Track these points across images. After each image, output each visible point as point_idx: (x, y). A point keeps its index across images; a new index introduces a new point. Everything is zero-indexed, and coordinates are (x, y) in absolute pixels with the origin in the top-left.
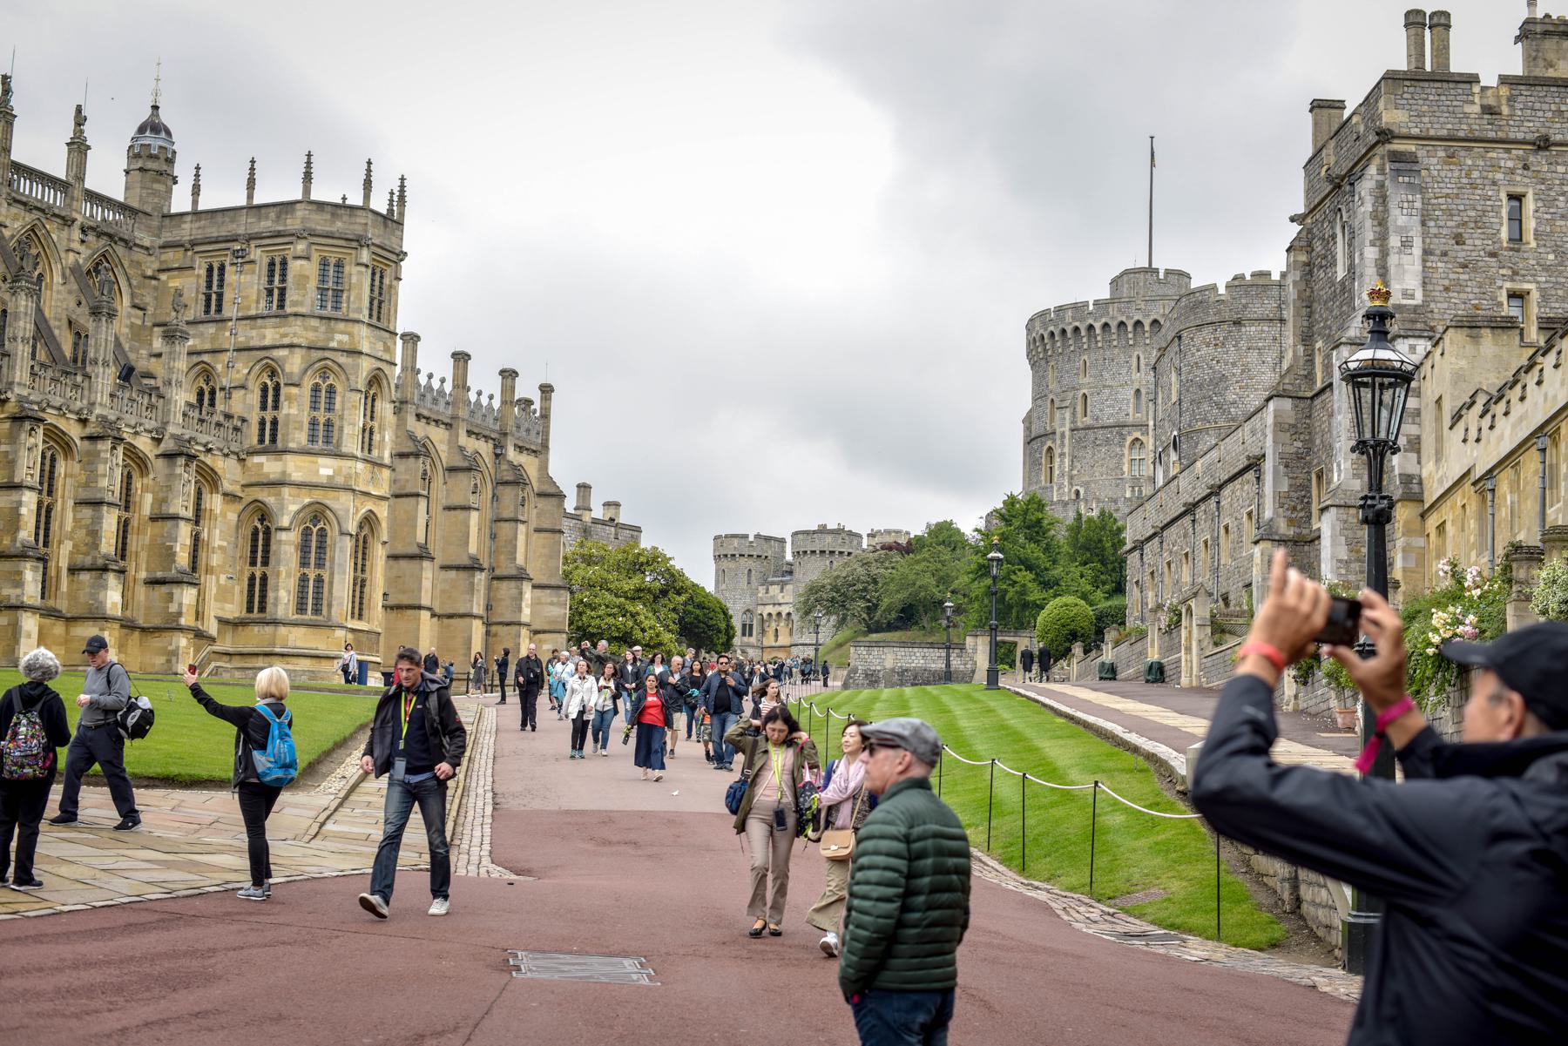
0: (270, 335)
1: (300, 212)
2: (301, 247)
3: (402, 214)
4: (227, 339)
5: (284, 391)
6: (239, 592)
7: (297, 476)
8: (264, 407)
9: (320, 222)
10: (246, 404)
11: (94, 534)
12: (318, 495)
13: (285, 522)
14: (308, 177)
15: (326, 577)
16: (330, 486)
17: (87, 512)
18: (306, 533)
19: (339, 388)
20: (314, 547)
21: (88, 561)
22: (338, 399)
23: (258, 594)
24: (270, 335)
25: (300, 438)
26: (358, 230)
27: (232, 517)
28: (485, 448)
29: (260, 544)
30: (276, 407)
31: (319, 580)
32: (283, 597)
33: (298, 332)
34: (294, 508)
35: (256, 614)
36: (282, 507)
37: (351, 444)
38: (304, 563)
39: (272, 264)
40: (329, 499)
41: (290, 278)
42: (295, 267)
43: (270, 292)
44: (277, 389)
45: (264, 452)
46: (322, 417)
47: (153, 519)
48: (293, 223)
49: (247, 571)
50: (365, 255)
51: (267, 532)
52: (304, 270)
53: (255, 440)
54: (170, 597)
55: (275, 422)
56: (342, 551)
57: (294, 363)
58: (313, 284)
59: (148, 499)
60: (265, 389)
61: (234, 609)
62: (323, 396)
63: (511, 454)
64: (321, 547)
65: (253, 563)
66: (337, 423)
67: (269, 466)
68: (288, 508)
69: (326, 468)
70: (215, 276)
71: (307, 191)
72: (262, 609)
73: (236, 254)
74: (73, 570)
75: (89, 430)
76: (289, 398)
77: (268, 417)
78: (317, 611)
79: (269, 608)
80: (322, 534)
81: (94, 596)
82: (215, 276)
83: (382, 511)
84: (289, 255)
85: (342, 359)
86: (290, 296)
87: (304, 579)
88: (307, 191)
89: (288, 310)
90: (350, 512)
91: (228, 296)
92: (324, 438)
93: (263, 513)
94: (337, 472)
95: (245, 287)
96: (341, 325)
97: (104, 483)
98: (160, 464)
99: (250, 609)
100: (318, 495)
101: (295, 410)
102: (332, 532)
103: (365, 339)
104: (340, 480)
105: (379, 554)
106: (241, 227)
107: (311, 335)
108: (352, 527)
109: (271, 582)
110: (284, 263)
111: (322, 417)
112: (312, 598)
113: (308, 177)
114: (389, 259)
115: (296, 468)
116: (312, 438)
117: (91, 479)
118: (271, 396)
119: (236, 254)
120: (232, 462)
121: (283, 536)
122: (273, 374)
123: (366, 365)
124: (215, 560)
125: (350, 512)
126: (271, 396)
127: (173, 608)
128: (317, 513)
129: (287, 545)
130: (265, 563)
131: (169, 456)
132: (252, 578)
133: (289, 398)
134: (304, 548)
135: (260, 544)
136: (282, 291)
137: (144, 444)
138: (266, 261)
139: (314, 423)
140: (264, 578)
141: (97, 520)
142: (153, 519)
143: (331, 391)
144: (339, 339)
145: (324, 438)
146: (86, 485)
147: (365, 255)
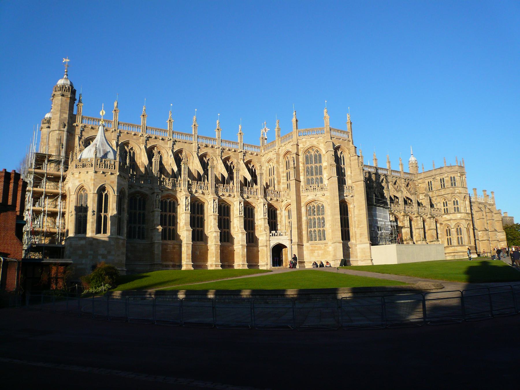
0: (443, 192)
1: (444, 169)
2: (446, 175)
5: (448, 202)
8: (444, 206)
10: (441, 206)
11: (420, 234)
12: (458, 221)
13: (453, 227)
18: (457, 229)
19: (458, 200)
20: (459, 231)
23: (449, 241)
24: (443, 193)
26: (457, 170)
31: (461, 237)
32: (455, 242)
33: (448, 191)
37: (463, 211)
38: (458, 235)
40: (461, 221)
44: (446, 202)
45: (446, 214)
46: (456, 206)
47: (429, 230)
49: (447, 237)
51: (449, 230)
53: (443, 212)
56: (464, 231)
60: (444, 203)
61: (446, 244)
62: (456, 203)
64: (461, 231)
67: (447, 217)
68: (453, 224)
69: (459, 216)
70: (430, 184)
72: (451, 244)
73: (433, 179)
75: (415, 216)
76: (449, 204)
78: (462, 243)
80: (460, 228)
82: (430, 184)
85: (458, 194)
86: (445, 185)
87: (458, 237)
92: (457, 210)
96: (457, 188)
97: (420, 225)
98: (428, 219)
99: (448, 244)
101: (450, 206)
107: (451, 192)
111: (456, 206)
116: (455, 211)
117: (417, 224)
119: (433, 179)
123: (463, 195)
129: (454, 231)
130: (450, 235)
131: (430, 218)
132: (448, 239)
133: (449, 204)
135: (448, 232)
136: (444, 184)
139: (455, 208)
140: (450, 239)
142: (429, 230)
143: (457, 201)
145: (457, 210)
146: (417, 226)
147: (459, 175)
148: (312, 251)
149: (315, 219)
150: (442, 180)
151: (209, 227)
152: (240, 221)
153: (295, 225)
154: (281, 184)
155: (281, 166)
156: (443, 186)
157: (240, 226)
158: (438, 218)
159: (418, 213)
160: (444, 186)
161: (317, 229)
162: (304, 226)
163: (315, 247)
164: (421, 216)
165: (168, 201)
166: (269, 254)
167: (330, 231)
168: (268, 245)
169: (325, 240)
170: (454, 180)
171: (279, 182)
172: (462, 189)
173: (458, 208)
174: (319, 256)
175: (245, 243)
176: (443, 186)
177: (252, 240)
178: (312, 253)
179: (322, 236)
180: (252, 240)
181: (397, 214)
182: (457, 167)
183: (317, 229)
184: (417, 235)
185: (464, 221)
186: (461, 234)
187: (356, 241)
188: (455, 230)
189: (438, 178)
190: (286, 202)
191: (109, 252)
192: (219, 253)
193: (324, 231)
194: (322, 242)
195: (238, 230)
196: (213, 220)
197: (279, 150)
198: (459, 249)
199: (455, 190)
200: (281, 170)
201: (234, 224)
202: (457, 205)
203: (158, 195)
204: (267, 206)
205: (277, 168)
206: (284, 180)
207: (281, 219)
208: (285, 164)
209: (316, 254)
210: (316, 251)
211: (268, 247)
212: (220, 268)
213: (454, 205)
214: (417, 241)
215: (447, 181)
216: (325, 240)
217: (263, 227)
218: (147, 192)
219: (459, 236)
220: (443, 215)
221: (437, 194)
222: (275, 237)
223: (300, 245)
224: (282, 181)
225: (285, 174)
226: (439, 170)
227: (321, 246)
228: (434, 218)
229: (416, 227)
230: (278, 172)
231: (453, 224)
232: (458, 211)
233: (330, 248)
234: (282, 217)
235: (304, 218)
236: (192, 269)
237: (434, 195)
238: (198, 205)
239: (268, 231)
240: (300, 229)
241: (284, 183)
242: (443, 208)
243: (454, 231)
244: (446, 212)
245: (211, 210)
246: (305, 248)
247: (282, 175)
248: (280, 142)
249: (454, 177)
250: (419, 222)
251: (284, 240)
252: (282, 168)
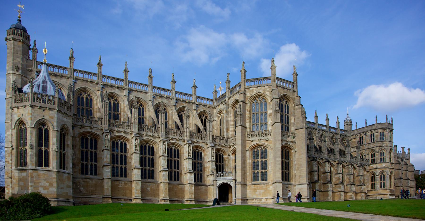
0: (372, 146)
1: (376, 125)
2: (376, 131)
3: (392, 123)
4: (364, 148)
5: (375, 154)
7: (379, 167)
8: (372, 157)
9: (379, 126)
10: (369, 157)
11: (350, 179)
12: (383, 169)
13: (378, 174)
14: (376, 120)
15: (385, 182)
16: (385, 168)
17: (348, 176)
18: (381, 176)
19: (385, 152)
20: (382, 178)
21: (349, 184)
22: (385, 154)
23: (373, 186)
24: (372, 146)
25: (379, 161)
27: (368, 175)
29: (373, 178)
30: (374, 157)
32: (378, 186)
33: (377, 144)
34: (379, 172)
35: (373, 189)
36: (377, 172)
37: (388, 161)
38: (381, 180)
39: (371, 135)
40: (385, 170)
41: (375, 136)
42: (375, 134)
43: (371, 139)
44: (374, 154)
46: (382, 157)
47: (357, 176)
48: (374, 127)
51: (374, 177)
52: (377, 134)
54: (361, 188)
55: (374, 159)
56: (387, 178)
57: (377, 149)
58: (379, 136)
59: (356, 173)
60: (372, 154)
61: (370, 188)
62: (382, 154)
64: (384, 177)
65: (372, 181)
66: (385, 158)
67: (374, 166)
68: (378, 172)
69: (384, 165)
71: (376, 122)
72: (374, 188)
74: (347, 185)
76: (377, 155)
77: (373, 158)
78: (384, 187)
79: (376, 188)
80: (384, 175)
81: (351, 189)
83: (393, 171)
84: (374, 133)
85: (385, 147)
86: (375, 139)
87: (381, 183)
88: (376, 122)
89: (375, 141)
90: (388, 171)
91: (364, 141)
93: (373, 173)
94: (386, 165)
95: (367, 139)
96: (385, 142)
97: (351, 172)
98: (357, 168)
99: (372, 188)
100: (383, 169)
101: (377, 156)
102: (386, 175)
103: (388, 143)
104: (386, 167)
105: (393, 177)
106: (365, 130)
107: (379, 145)
109: (376, 184)
110: (373, 134)
111: (382, 157)
112: (383, 186)
113: (376, 120)
114: (391, 130)
115: (379, 166)
116: (381, 161)
118: (373, 155)
120: (368, 166)
121: (377, 176)
122: (373, 151)
123: (389, 148)
126: (373, 155)
127: (362, 189)
128: (382, 172)
129: (378, 178)
130: (374, 181)
131: (359, 166)
132: (372, 184)
133: (377, 155)
134: (381, 178)
135: (373, 178)
136: (374, 139)
138: (370, 134)
139: (381, 159)
140: (374, 183)
141: (350, 177)
142: (357, 176)
143: (384, 153)
144: (385, 144)
145: (383, 160)
146: (348, 172)
147: (388, 130)
148: (255, 190)
149: (258, 162)
150: (372, 136)
151: (160, 167)
152: (189, 161)
153: (239, 168)
154: (230, 132)
155: (230, 115)
156: (372, 140)
157: (189, 166)
158: (366, 167)
159: (350, 162)
160: (374, 140)
161: (260, 171)
162: (248, 168)
163: (257, 187)
164: (352, 165)
165: (120, 142)
166: (215, 192)
167: (272, 172)
168: (215, 184)
169: (266, 180)
170: (383, 135)
171: (228, 130)
172: (389, 142)
173: (384, 158)
174: (260, 194)
175: (193, 182)
176: (372, 140)
177: (199, 179)
178: (255, 192)
179: (264, 177)
180: (199, 179)
181: (332, 162)
182: (387, 124)
183: (260, 171)
184: (347, 180)
185: (388, 169)
186: (384, 180)
187: (295, 182)
188: (379, 176)
189: (369, 134)
190: (233, 147)
192: (168, 190)
193: (266, 173)
194: (264, 182)
195: (187, 170)
196: (162, 161)
197: (228, 101)
198: (381, 192)
199: (383, 144)
200: (230, 119)
201: (184, 165)
202: (384, 155)
203: (107, 135)
204: (214, 150)
205: (226, 117)
206: (232, 128)
207: (228, 162)
208: (233, 113)
209: (258, 193)
210: (258, 190)
211: (215, 186)
212: (168, 203)
213: (381, 156)
214: (347, 185)
215: (377, 136)
216: (266, 180)
217: (211, 168)
218: (98, 133)
219: (382, 182)
220: (371, 164)
221: (367, 147)
222: (222, 177)
223: (244, 185)
224: (230, 129)
225: (233, 123)
226: (371, 127)
227: (263, 185)
228: (363, 166)
229: (347, 174)
230: (227, 121)
231: (378, 172)
232: (384, 160)
233: (271, 187)
234: (229, 160)
235: (249, 161)
236: (141, 202)
237: (364, 148)
238: (149, 147)
239: (215, 172)
240: (244, 171)
241: (232, 131)
242: (370, 159)
243: (378, 178)
244: (374, 162)
245: (161, 151)
246: (248, 187)
247: (231, 123)
248: (229, 93)
249: (383, 133)
250: (350, 170)
251: (228, 179)
252: (231, 118)
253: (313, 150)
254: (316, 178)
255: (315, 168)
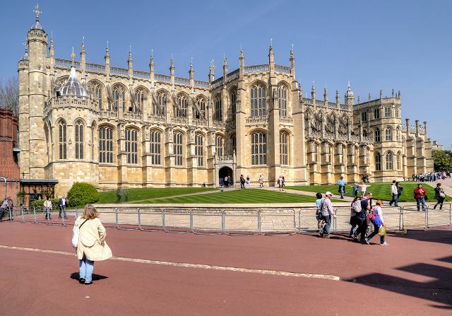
0: (376, 123)
6: (375, 167)
11: (351, 160)
12: (389, 149)
14: (381, 94)
24: (376, 123)
28: (414, 135)
29: (378, 158)
31: (390, 164)
32: (384, 167)
40: (391, 149)
46: (388, 135)
50: (394, 106)
63: (419, 136)
69: (390, 144)
108: (396, 154)
111: (388, 135)
112: (390, 166)
113: (381, 94)
123: (396, 125)
124: (370, 162)
125: (395, 151)
128: (389, 152)
134: (387, 158)
137: (357, 144)
144: (390, 121)
191: (86, 174)
253: (310, 130)
254: (313, 159)
255: (313, 150)
